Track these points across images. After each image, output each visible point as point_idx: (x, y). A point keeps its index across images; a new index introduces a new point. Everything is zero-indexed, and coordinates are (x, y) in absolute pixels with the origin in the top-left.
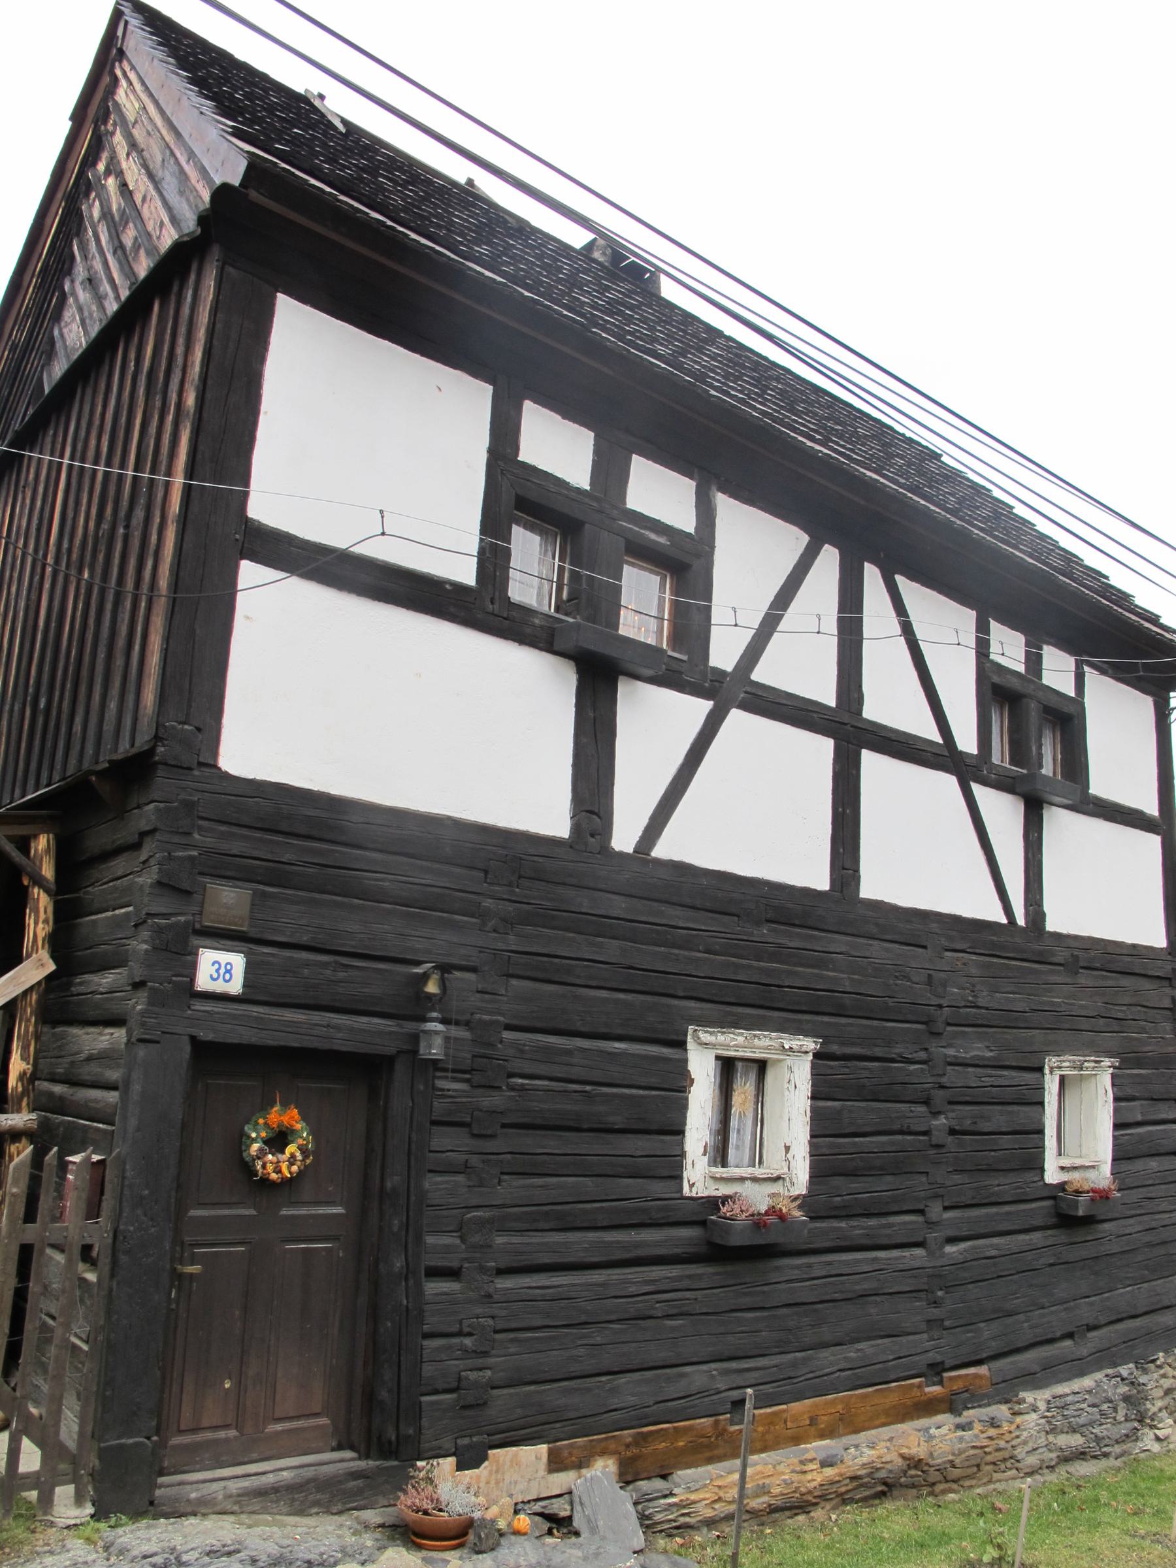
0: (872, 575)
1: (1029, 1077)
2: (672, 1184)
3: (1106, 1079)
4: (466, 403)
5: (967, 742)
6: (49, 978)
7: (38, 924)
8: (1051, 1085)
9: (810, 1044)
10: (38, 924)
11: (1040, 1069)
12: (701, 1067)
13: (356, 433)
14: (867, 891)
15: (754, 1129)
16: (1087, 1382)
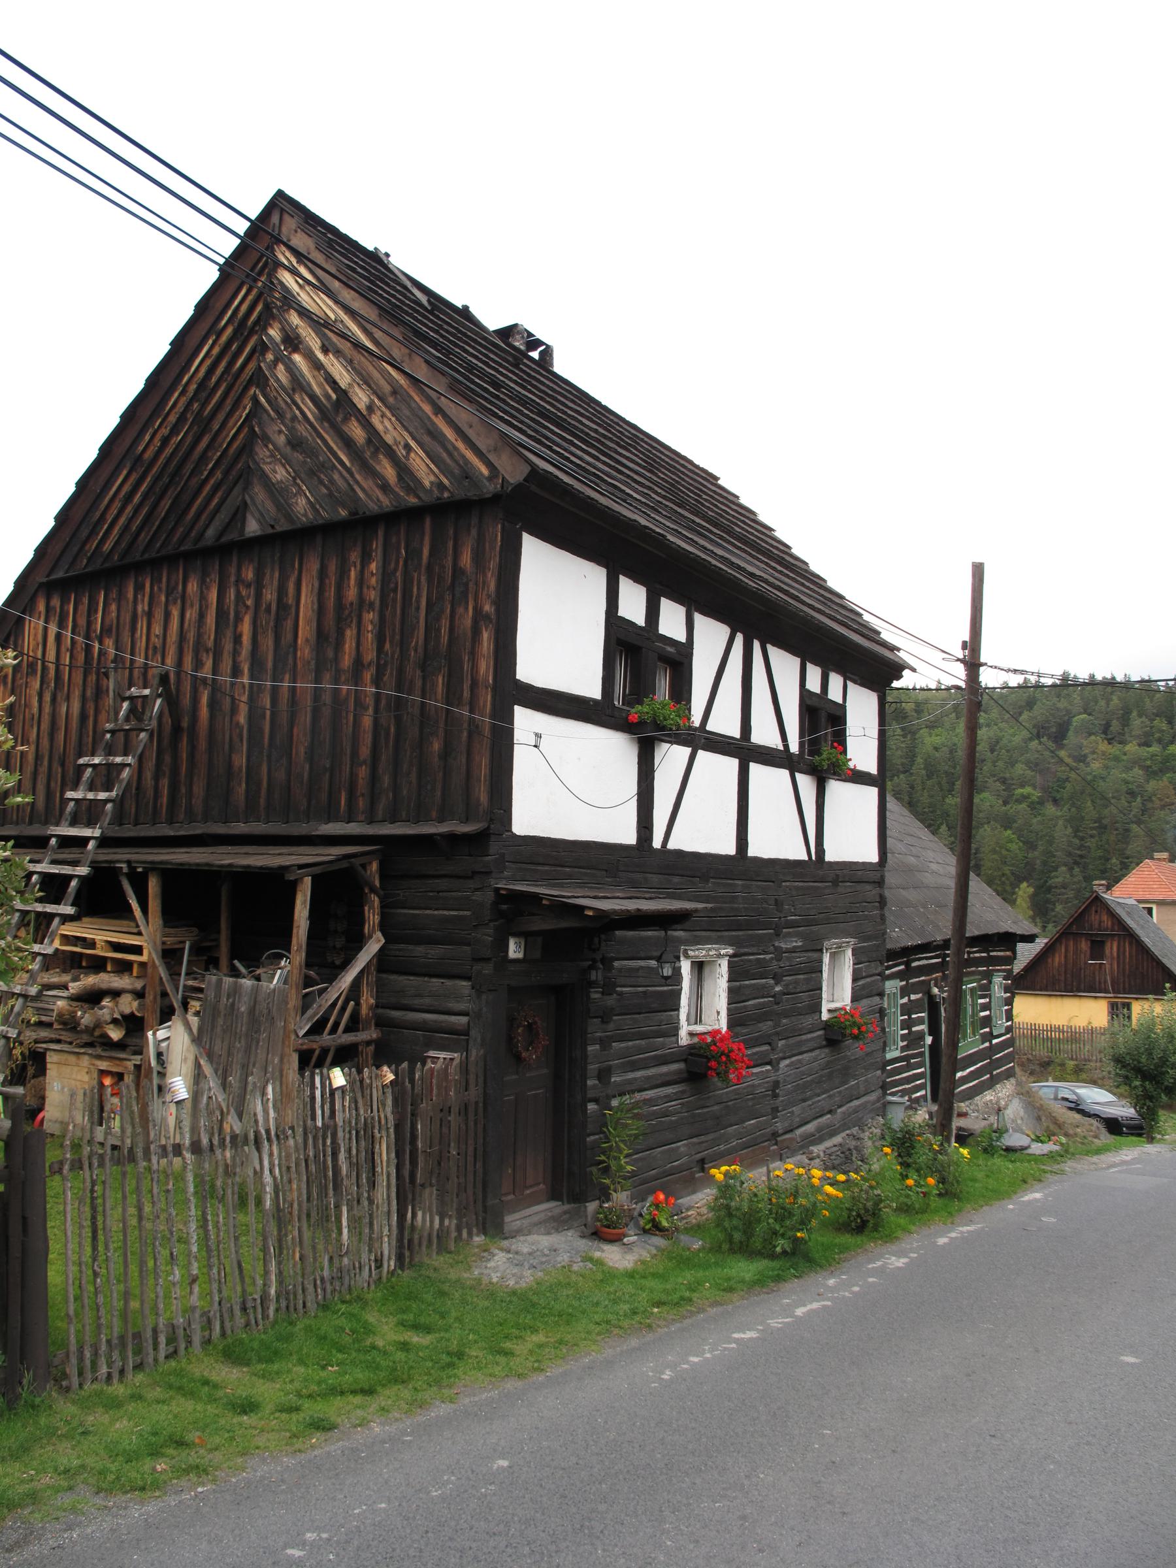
0: (757, 645)
1: (815, 955)
2: (674, 1039)
3: (849, 952)
4: (594, 577)
5: (794, 748)
6: (381, 950)
7: (372, 917)
8: (826, 959)
9: (730, 951)
10: (372, 917)
11: (821, 950)
12: (686, 967)
13: (561, 615)
14: (752, 852)
15: (706, 1003)
16: (838, 1139)
